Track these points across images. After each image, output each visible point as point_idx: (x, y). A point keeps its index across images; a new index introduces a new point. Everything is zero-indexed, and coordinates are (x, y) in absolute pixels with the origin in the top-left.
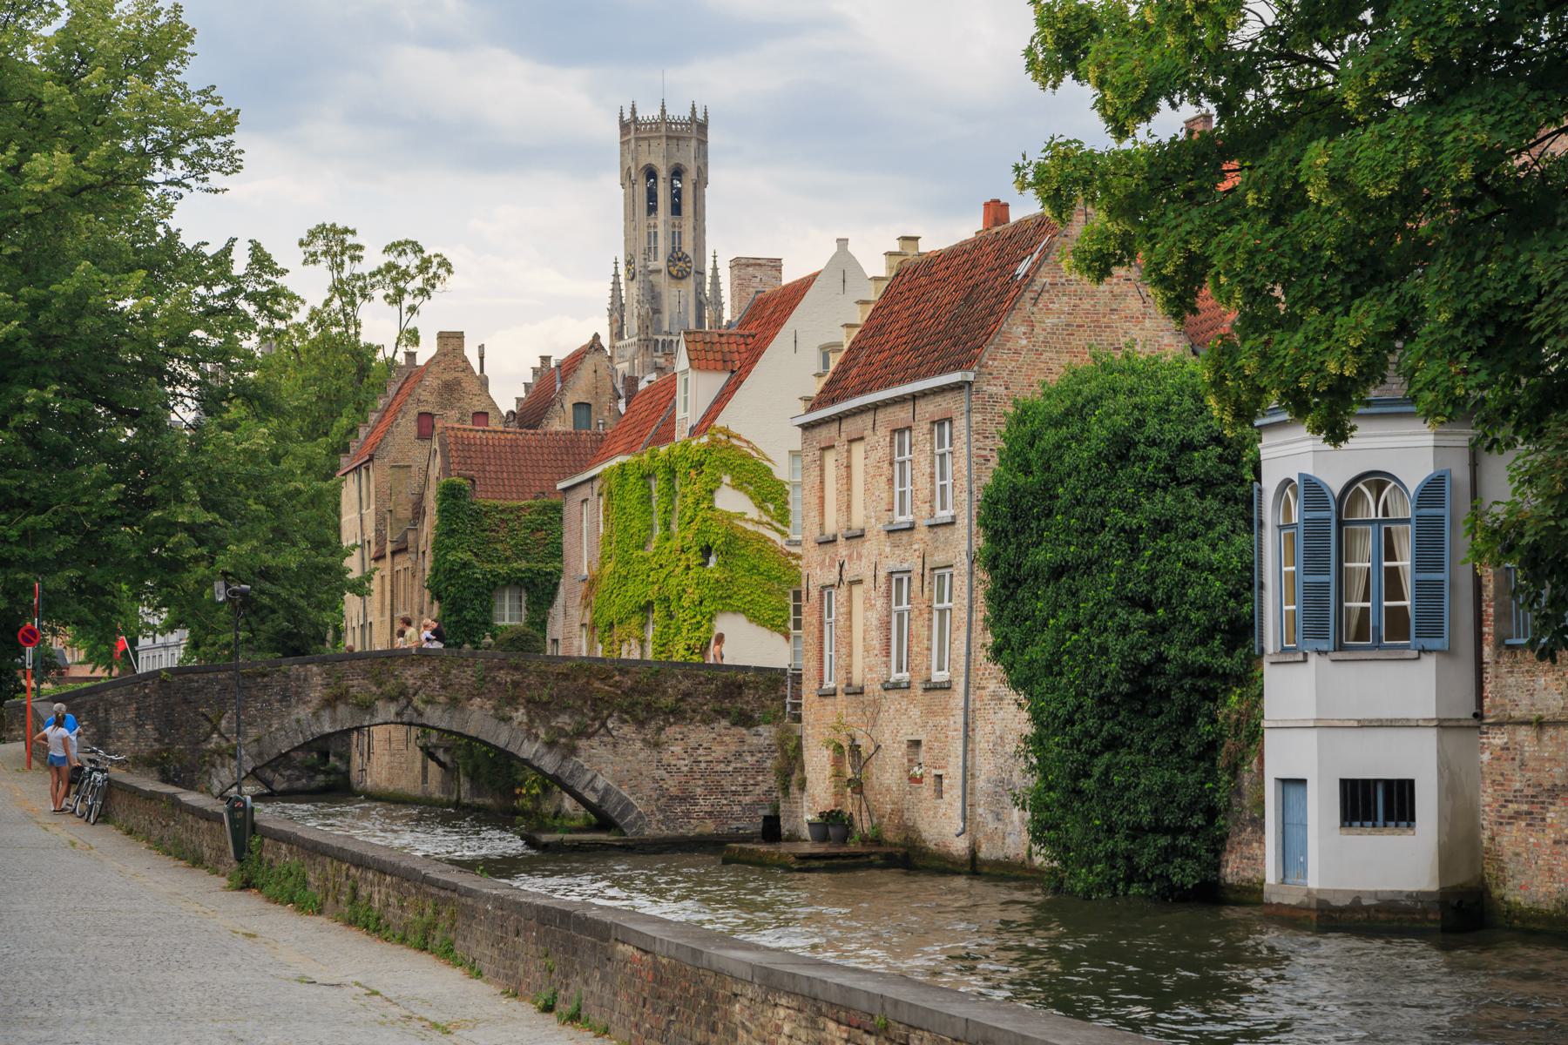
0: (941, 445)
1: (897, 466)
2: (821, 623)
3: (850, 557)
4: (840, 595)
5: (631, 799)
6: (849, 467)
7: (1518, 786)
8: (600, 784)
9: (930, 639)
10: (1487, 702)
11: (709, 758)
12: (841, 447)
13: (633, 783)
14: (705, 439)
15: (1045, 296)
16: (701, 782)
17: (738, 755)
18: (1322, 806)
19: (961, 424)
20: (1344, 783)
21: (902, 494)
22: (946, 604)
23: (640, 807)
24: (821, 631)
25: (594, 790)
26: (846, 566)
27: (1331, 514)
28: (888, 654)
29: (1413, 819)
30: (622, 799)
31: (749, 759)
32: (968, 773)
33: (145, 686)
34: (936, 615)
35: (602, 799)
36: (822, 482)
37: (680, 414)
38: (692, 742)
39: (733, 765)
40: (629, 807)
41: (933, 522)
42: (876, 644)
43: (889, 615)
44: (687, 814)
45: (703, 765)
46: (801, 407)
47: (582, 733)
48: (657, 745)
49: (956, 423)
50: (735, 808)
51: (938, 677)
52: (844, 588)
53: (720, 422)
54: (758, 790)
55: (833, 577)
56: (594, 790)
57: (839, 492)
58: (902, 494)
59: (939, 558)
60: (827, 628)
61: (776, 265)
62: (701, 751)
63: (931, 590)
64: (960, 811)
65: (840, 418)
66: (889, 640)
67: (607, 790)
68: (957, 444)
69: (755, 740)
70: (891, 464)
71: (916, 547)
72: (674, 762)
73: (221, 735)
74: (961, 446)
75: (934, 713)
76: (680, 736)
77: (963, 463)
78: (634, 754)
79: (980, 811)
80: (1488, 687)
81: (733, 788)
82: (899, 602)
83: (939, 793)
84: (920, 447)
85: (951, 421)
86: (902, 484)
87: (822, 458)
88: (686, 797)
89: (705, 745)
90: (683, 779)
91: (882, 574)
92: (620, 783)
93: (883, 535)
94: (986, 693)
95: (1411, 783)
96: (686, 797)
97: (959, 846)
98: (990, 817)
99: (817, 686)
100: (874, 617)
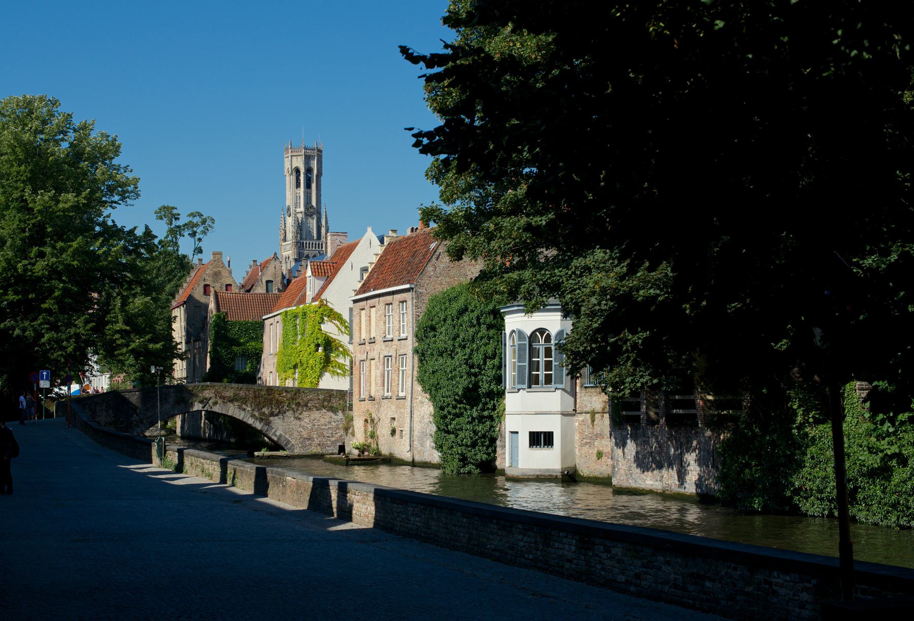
0: (403, 310)
1: (387, 317)
2: (360, 374)
3: (370, 350)
4: (366, 364)
5: (290, 439)
6: (370, 317)
7: (586, 434)
8: (278, 433)
9: (398, 381)
10: (577, 406)
12: (367, 308)
14: (317, 303)
15: (440, 256)
18: (524, 439)
19: (409, 303)
20: (530, 433)
21: (389, 327)
22: (404, 368)
23: (293, 442)
24: (360, 377)
25: (275, 435)
26: (369, 353)
27: (527, 342)
28: (384, 386)
29: (553, 445)
30: (286, 439)
32: (411, 430)
33: (109, 397)
34: (401, 372)
35: (279, 439)
36: (360, 322)
37: (308, 293)
38: (312, 418)
40: (288, 442)
41: (399, 338)
42: (380, 382)
43: (384, 372)
44: (310, 445)
45: (316, 426)
46: (353, 293)
47: (272, 414)
48: (299, 419)
49: (408, 302)
50: (328, 442)
51: (401, 394)
53: (323, 297)
54: (337, 436)
55: (364, 357)
56: (275, 435)
57: (366, 325)
58: (389, 327)
59: (402, 352)
60: (362, 376)
63: (399, 363)
64: (409, 443)
65: (367, 299)
66: (384, 381)
67: (281, 435)
68: (408, 310)
69: (336, 417)
73: (137, 415)
74: (410, 311)
75: (400, 408)
77: (410, 317)
79: (416, 443)
80: (578, 401)
82: (388, 367)
83: (401, 437)
84: (395, 310)
85: (406, 301)
86: (389, 324)
87: (360, 313)
91: (382, 357)
92: (286, 433)
94: (418, 400)
95: (552, 432)
97: (407, 457)
98: (419, 445)
100: (379, 372)
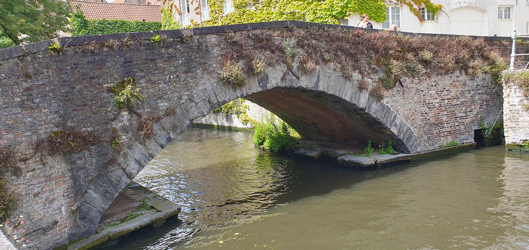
11: (449, 97)
16: (446, 113)
17: (462, 93)
31: (468, 95)
38: (440, 87)
39: (461, 100)
45: (446, 101)
62: (445, 93)
72: (432, 101)
76: (434, 84)
81: (461, 115)
88: (439, 124)
89: (447, 88)
90: (437, 112)
96: (439, 124)
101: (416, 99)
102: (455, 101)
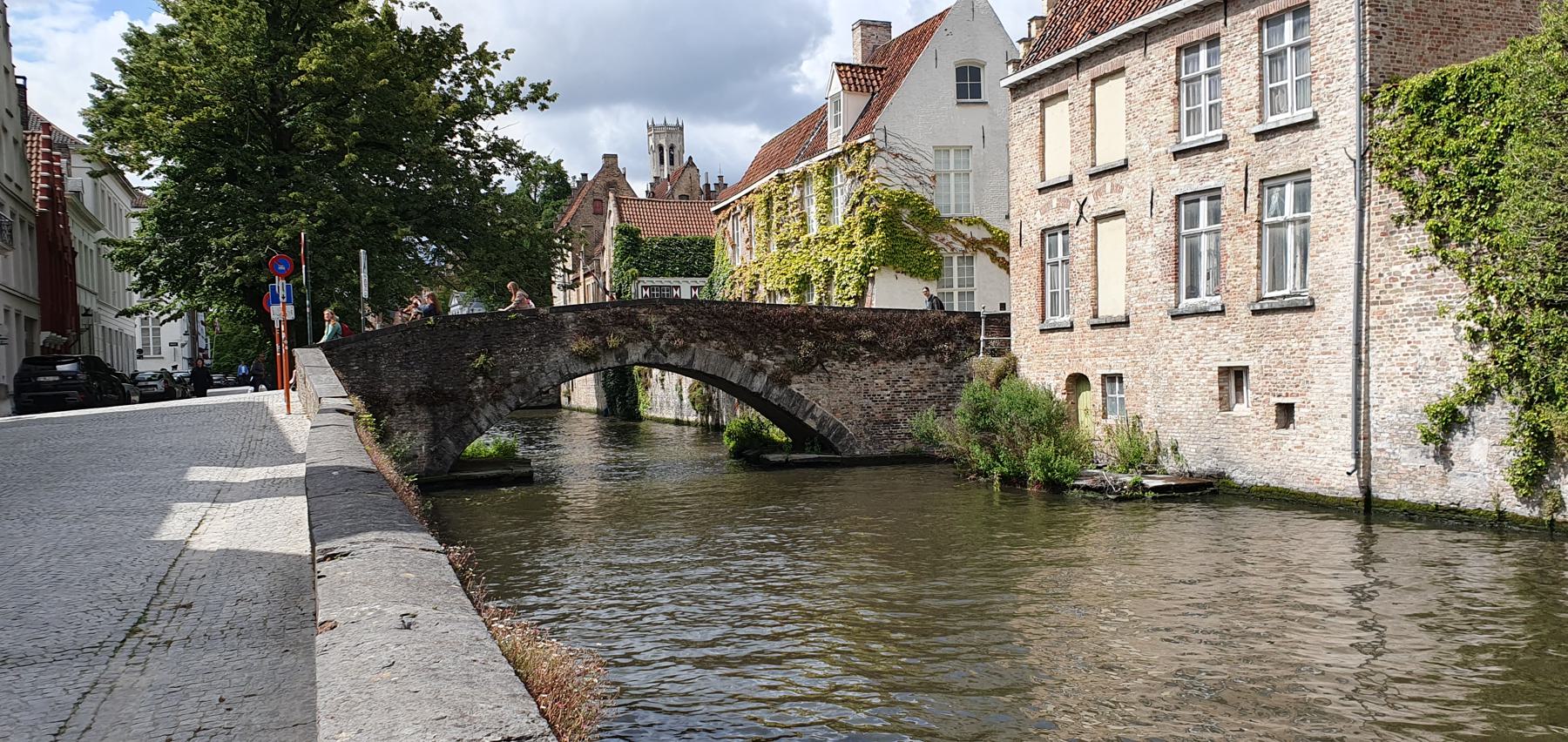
8: (818, 414)
11: (908, 389)
13: (845, 410)
17: (932, 386)
25: (814, 417)
28: (1177, 280)
31: (941, 388)
35: (819, 425)
36: (1043, 132)
37: (831, 129)
38: (893, 376)
40: (842, 432)
44: (890, 436)
52: (1086, 227)
53: (879, 122)
56: (814, 417)
61: (887, 26)
62: (901, 383)
66: (1177, 264)
70: (1177, 83)
71: (1231, 160)
78: (845, 387)
88: (890, 422)
89: (904, 378)
90: (886, 407)
91: (1165, 201)
93: (1165, 160)
99: (1037, 321)
101: (852, 388)
102: (919, 394)
